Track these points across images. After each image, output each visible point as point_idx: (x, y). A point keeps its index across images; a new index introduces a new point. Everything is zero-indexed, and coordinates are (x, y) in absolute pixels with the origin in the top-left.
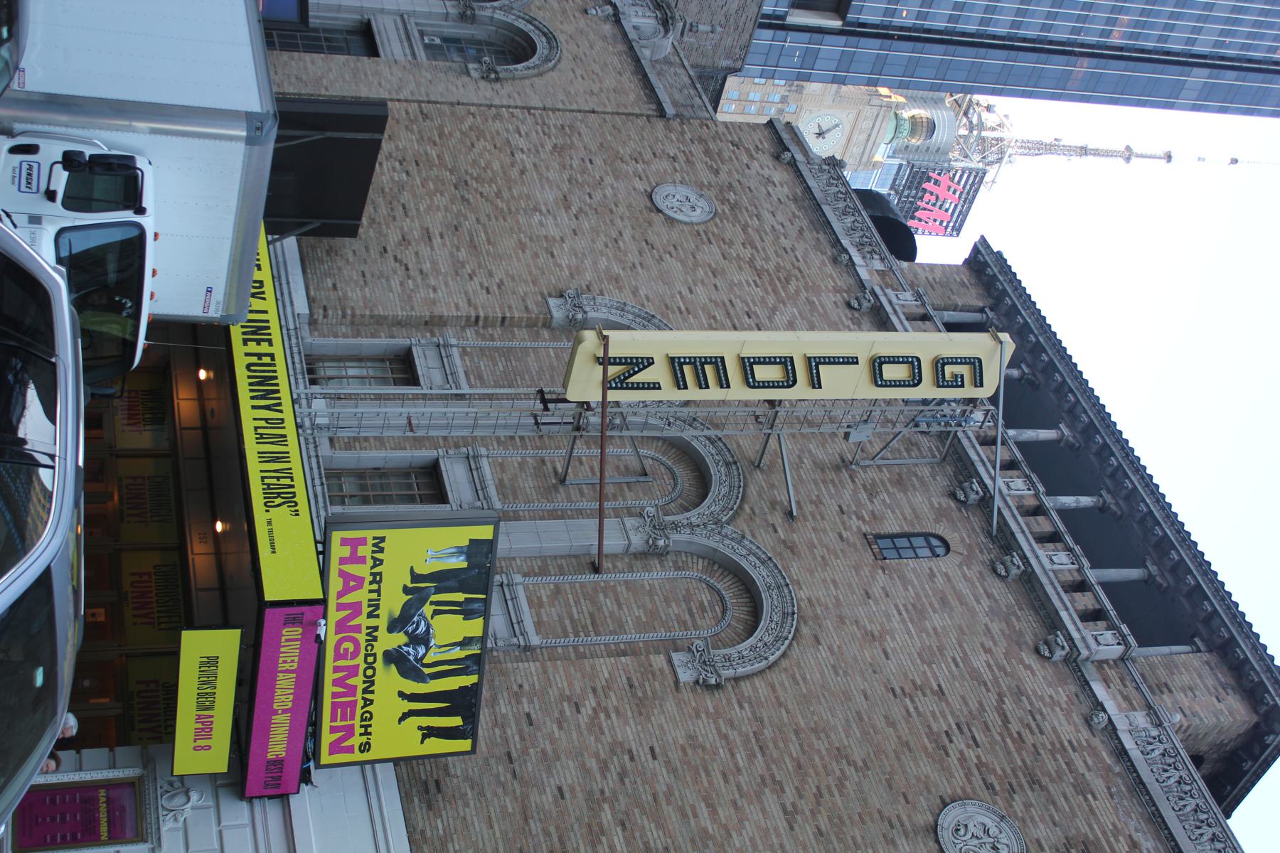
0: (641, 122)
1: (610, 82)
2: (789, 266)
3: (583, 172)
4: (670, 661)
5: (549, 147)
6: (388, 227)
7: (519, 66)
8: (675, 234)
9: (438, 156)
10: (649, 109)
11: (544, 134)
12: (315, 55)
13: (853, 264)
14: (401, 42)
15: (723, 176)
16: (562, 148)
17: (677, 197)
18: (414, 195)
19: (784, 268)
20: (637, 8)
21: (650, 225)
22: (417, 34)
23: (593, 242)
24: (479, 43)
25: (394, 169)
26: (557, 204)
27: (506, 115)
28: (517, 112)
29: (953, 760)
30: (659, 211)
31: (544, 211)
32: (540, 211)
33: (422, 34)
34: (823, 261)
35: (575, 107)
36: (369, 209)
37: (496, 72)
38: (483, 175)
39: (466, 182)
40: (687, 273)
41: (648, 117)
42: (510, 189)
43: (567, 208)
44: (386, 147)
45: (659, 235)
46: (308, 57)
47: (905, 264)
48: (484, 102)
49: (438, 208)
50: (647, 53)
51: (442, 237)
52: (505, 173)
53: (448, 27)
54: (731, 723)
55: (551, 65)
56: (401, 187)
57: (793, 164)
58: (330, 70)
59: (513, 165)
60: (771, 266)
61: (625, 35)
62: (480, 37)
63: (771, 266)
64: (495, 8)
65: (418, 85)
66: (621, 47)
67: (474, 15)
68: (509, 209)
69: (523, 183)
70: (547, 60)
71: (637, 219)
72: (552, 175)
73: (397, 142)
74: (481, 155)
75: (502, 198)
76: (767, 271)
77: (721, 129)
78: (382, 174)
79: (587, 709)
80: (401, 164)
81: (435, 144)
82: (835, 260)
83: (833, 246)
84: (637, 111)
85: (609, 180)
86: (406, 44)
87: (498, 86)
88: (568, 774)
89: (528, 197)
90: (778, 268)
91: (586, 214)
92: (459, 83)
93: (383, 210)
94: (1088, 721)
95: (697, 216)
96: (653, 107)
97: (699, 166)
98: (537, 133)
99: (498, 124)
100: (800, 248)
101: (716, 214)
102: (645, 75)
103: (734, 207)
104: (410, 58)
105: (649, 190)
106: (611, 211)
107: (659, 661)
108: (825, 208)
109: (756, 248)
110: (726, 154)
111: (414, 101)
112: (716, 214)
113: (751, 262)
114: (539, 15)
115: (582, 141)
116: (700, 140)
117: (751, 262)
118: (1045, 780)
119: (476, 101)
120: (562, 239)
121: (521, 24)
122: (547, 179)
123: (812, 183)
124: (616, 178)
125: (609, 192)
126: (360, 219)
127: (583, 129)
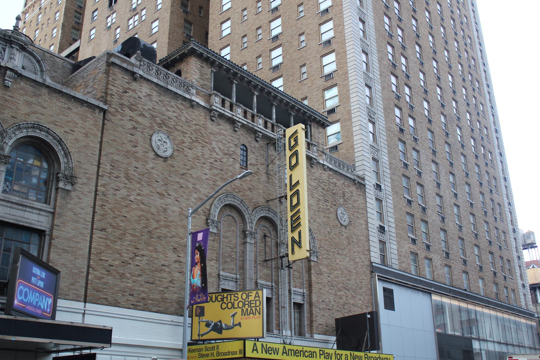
4: (313, 261)
14: (25, 211)
23: (182, 196)
26: (162, 199)
29: (332, 210)
31: (166, 207)
35: (98, 152)
40: (198, 170)
54: (324, 255)
57: (141, 77)
60: (195, 136)
63: (195, 136)
72: (145, 191)
79: (321, 287)
82: (192, 106)
86: (28, 209)
88: (332, 298)
94: (325, 170)
107: (312, 263)
108: (169, 87)
118: (334, 191)
122: (147, 194)
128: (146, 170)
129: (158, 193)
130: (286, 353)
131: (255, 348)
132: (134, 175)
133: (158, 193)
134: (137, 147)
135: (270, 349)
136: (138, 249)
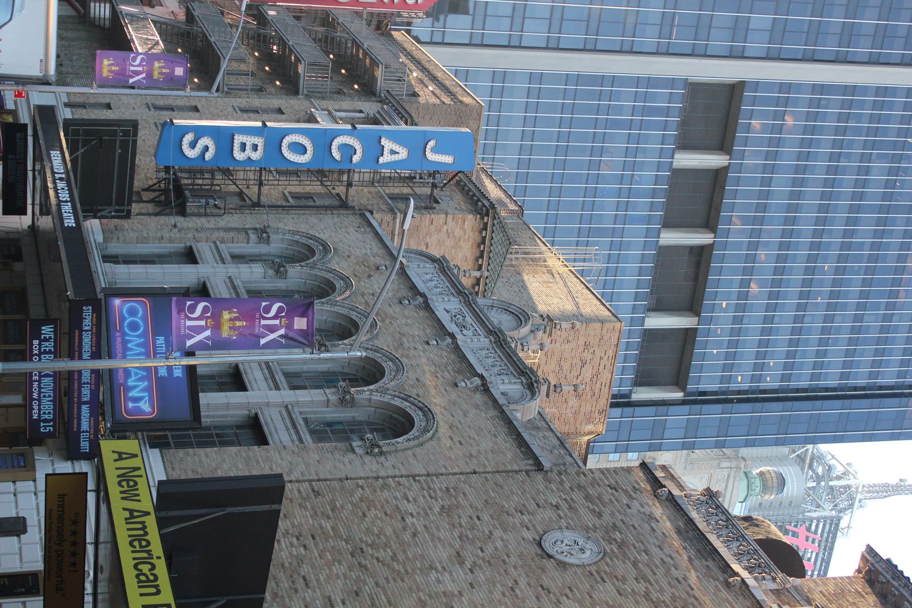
0: (521, 477)
1: (486, 444)
2: (684, 595)
3: (472, 528)
5: (437, 509)
6: (291, 599)
7: (399, 440)
8: (568, 577)
9: (333, 528)
10: (527, 464)
11: (431, 498)
12: (208, 450)
13: (747, 586)
14: (288, 429)
15: (606, 517)
16: (449, 509)
17: (566, 542)
18: (313, 567)
19: (680, 598)
20: (502, 377)
21: (543, 570)
22: (301, 422)
23: (491, 592)
24: (360, 423)
25: (292, 545)
27: (393, 485)
28: (403, 480)
30: (550, 557)
31: (440, 568)
32: (436, 569)
33: (306, 420)
34: (716, 586)
35: (456, 470)
36: (271, 584)
37: (379, 447)
38: (377, 541)
39: (362, 549)
41: (527, 472)
42: (404, 551)
43: (462, 563)
44: (282, 525)
45: (553, 579)
46: (201, 452)
47: (798, 581)
48: (370, 475)
49: (338, 577)
50: (519, 415)
51: (344, 603)
52: (397, 537)
53: (330, 412)
55: (429, 434)
56: (300, 561)
57: (671, 498)
58: (224, 461)
59: (404, 529)
61: (495, 401)
62: (360, 419)
64: (371, 391)
65: (308, 466)
66: (493, 413)
67: (353, 399)
68: (406, 571)
69: (416, 545)
70: (426, 430)
71: (530, 566)
72: (442, 534)
73: (294, 518)
74: (373, 523)
75: (397, 561)
76: (664, 602)
77: (597, 475)
78: (281, 550)
80: (298, 539)
81: (328, 517)
82: (728, 585)
83: (724, 572)
84: (516, 467)
85: (498, 533)
86: (292, 431)
87: (382, 459)
89: (422, 557)
90: (674, 598)
91: (480, 567)
92: (346, 460)
93: (285, 584)
95: (587, 557)
96: (531, 462)
97: (582, 511)
98: (424, 497)
99: (386, 494)
100: (693, 576)
101: (605, 553)
102: (519, 435)
103: (621, 545)
104: (297, 443)
105: (537, 538)
106: (504, 561)
108: (712, 538)
109: (649, 582)
110: (606, 498)
111: (304, 481)
112: (605, 553)
113: (647, 595)
114: (413, 392)
115: (468, 500)
116: (580, 487)
117: (647, 595)
119: (363, 475)
120: (460, 593)
121: (398, 402)
122: (439, 538)
123: (694, 514)
124: (505, 530)
125: (499, 544)
126: (264, 593)
127: (467, 489)
128: (490, 532)
129: (458, 553)
130: (132, 517)
131: (124, 456)
132: (460, 517)
133: (458, 553)
134: (522, 514)
135: (131, 483)
136: (314, 538)
